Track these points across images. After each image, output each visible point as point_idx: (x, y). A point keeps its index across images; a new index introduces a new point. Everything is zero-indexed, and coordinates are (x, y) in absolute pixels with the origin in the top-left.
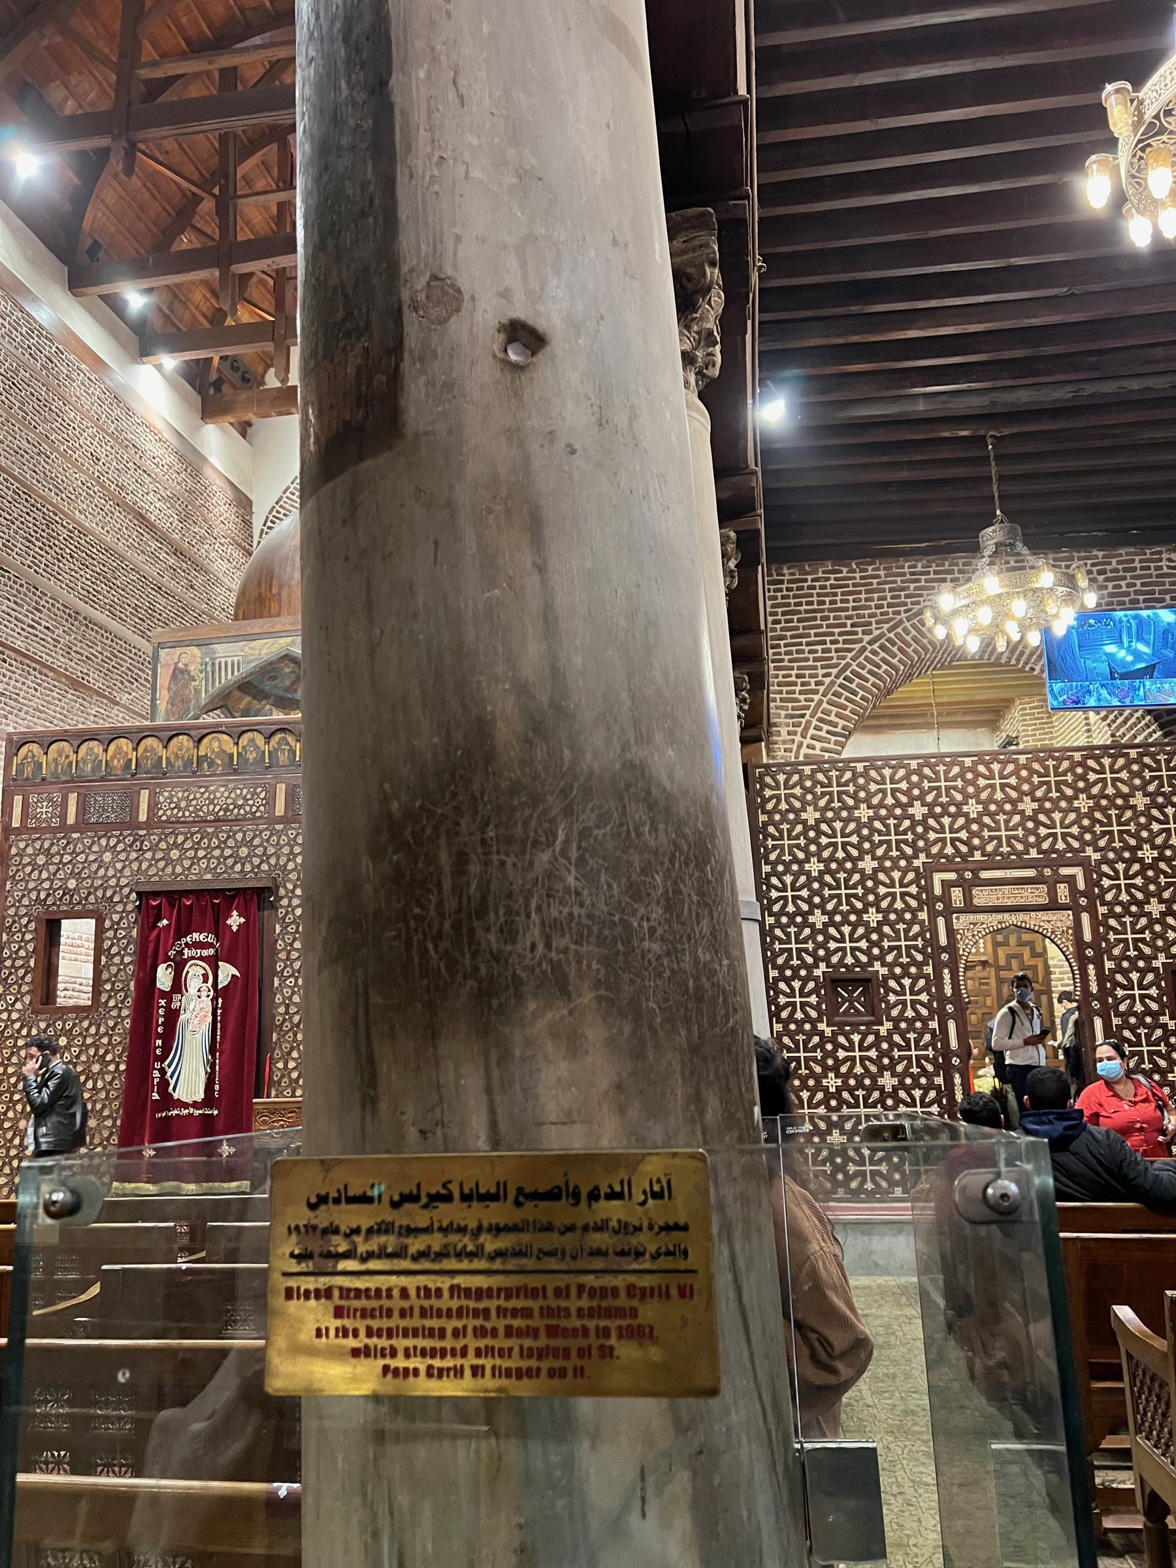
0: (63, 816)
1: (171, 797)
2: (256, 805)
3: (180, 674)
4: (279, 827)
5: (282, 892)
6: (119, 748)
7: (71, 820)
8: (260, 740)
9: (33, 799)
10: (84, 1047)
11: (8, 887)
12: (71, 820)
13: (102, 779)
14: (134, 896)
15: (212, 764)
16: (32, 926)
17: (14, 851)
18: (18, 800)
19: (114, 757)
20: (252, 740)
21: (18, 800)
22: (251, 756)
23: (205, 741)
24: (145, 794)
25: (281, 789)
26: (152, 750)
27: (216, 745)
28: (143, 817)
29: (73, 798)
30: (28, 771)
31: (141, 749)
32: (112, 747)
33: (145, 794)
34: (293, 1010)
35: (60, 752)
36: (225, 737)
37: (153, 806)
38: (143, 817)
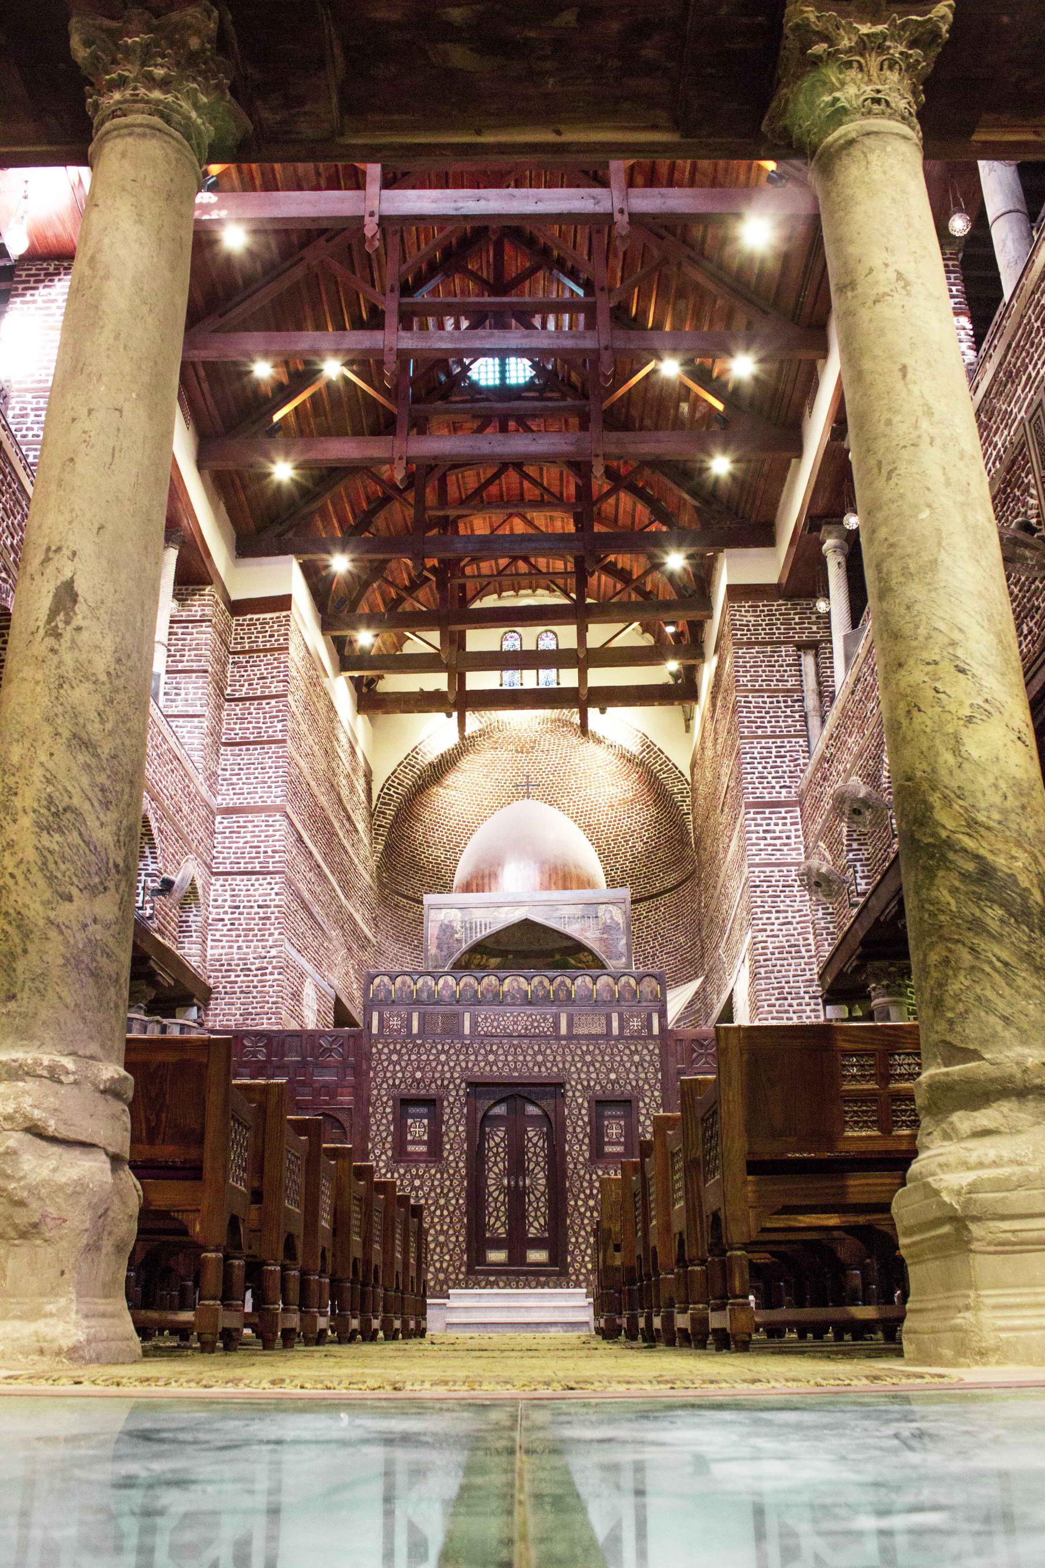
0: (409, 1027)
1: (486, 1018)
2: (546, 1027)
3: (447, 929)
4: (564, 1042)
5: (568, 1087)
6: (446, 982)
7: (415, 1030)
8: (546, 982)
9: (386, 1015)
10: (433, 1188)
11: (372, 1074)
12: (415, 1030)
13: (437, 1003)
14: (463, 1085)
15: (513, 997)
16: (391, 1103)
17: (374, 1050)
18: (375, 1016)
19: (443, 988)
20: (541, 983)
21: (375, 1016)
22: (541, 993)
23: (507, 981)
24: (467, 1016)
25: (615, 1017)
26: (471, 986)
27: (515, 984)
28: (467, 1031)
29: (415, 1016)
30: (382, 995)
31: (462, 984)
32: (441, 982)
33: (467, 1016)
34: (579, 1166)
35: (404, 983)
36: (522, 979)
37: (474, 1024)
38: (467, 1031)
